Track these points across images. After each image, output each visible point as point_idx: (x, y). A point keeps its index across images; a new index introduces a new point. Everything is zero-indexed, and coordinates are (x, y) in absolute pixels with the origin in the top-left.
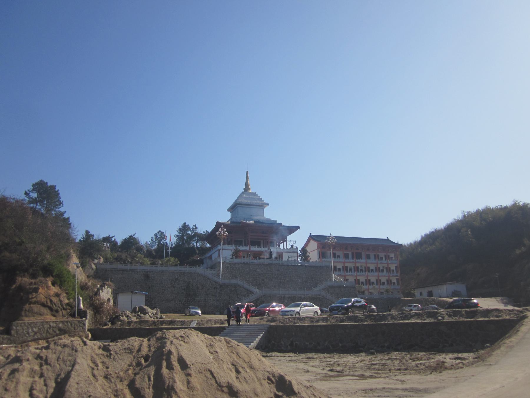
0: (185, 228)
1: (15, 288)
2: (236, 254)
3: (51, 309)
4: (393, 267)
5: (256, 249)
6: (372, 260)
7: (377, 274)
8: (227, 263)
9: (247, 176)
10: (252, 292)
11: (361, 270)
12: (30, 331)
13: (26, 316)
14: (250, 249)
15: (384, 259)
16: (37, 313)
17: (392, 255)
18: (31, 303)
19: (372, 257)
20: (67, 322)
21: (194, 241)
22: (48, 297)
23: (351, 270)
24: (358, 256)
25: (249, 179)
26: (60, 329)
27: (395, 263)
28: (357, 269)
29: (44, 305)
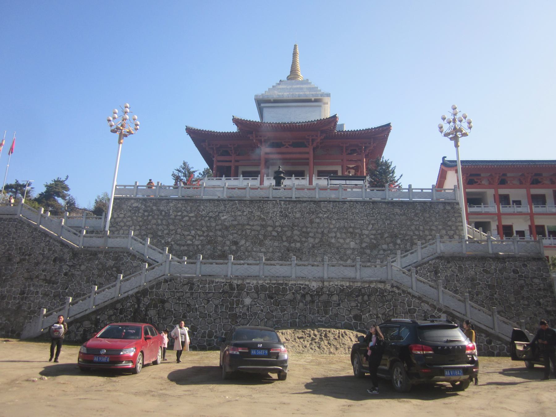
8: (137, 200)
9: (295, 54)
25: (298, 60)
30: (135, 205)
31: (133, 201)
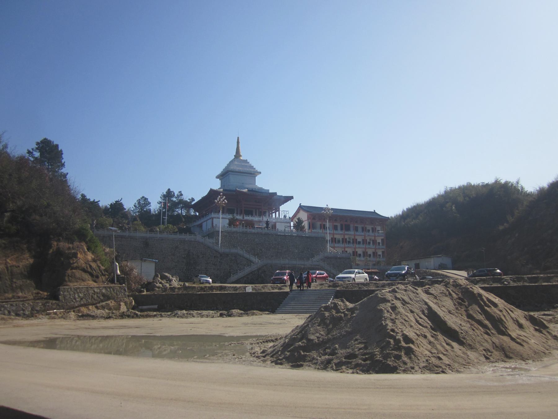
0: (169, 194)
1: (53, 252)
2: (232, 223)
3: (91, 275)
4: (379, 240)
5: (249, 218)
6: (360, 232)
7: (364, 246)
9: (238, 142)
10: (251, 262)
11: (349, 242)
12: (77, 296)
13: (70, 281)
14: (243, 218)
15: (371, 231)
16: (79, 279)
17: (379, 228)
18: (73, 268)
19: (360, 229)
20: (110, 288)
21: (178, 208)
22: (87, 262)
23: (339, 242)
24: (348, 228)
26: (104, 295)
27: (381, 236)
28: (344, 241)
29: (84, 271)
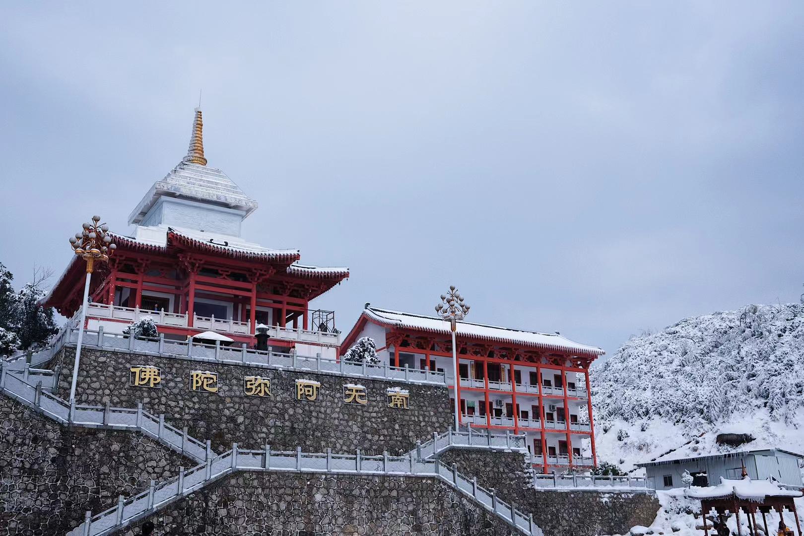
6: (526, 387)
8: (103, 353)
9: (199, 126)
11: (499, 413)
14: (191, 323)
19: (525, 378)
24: (495, 374)
30: (102, 359)
31: (98, 354)
